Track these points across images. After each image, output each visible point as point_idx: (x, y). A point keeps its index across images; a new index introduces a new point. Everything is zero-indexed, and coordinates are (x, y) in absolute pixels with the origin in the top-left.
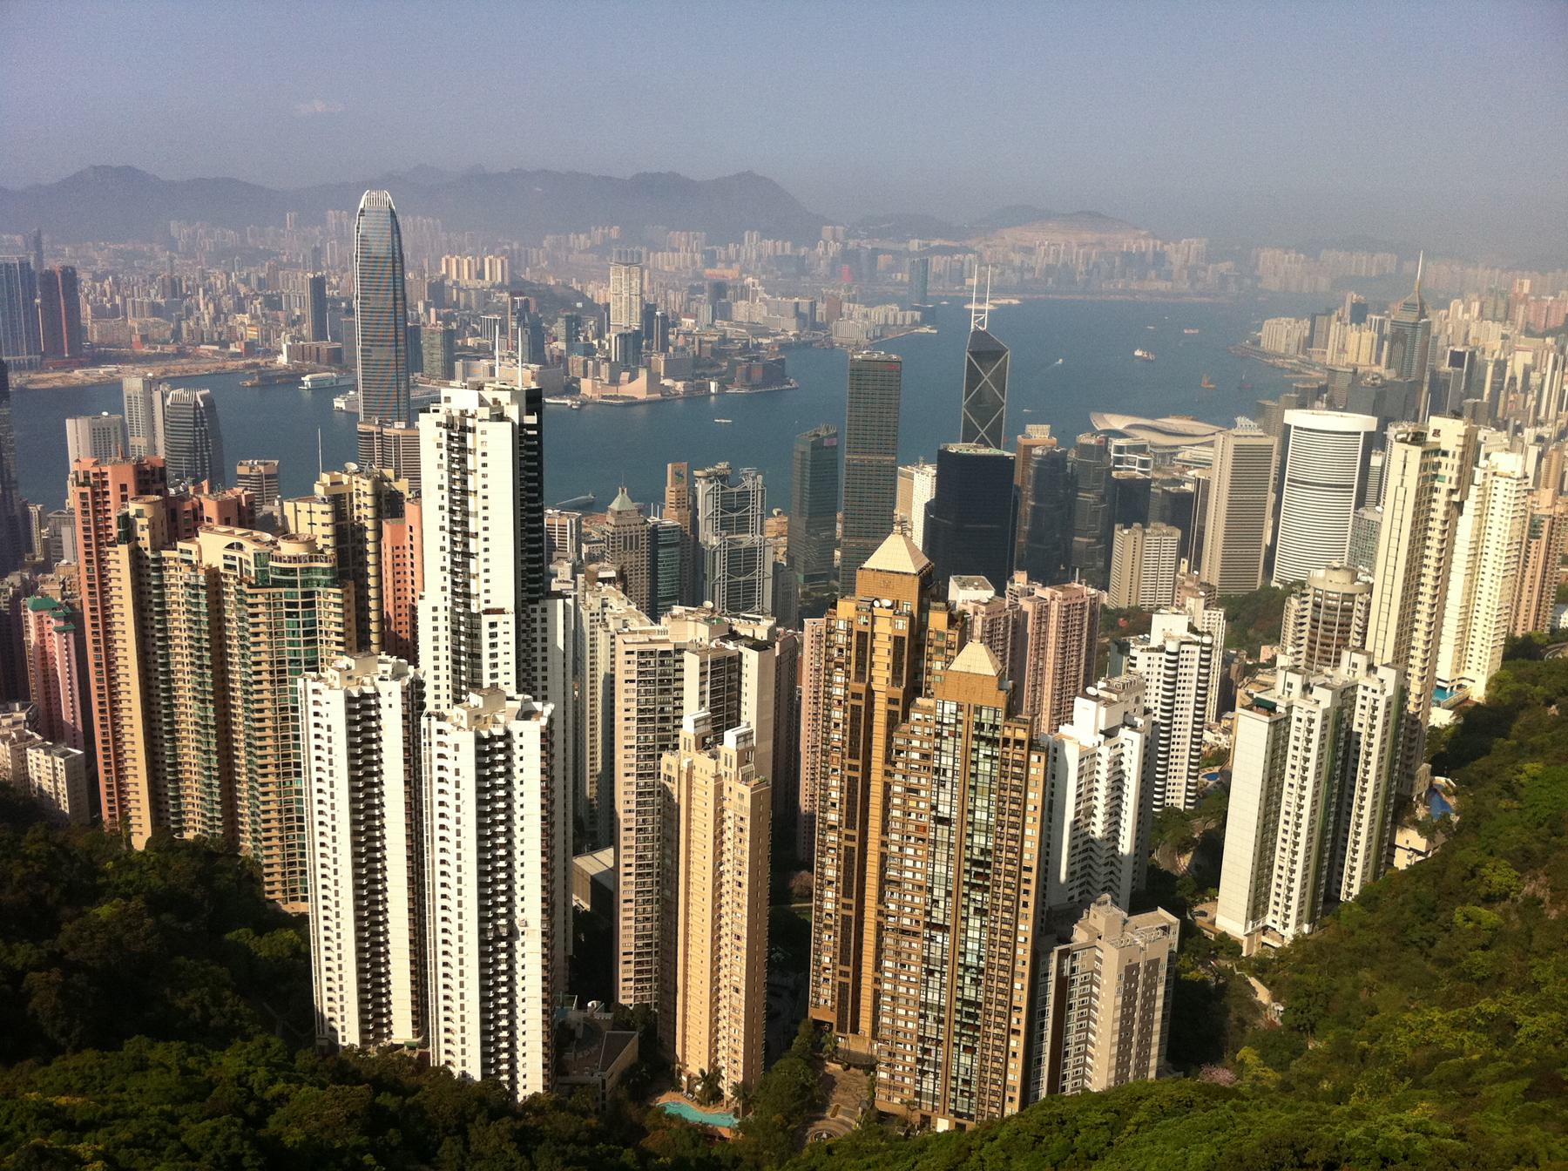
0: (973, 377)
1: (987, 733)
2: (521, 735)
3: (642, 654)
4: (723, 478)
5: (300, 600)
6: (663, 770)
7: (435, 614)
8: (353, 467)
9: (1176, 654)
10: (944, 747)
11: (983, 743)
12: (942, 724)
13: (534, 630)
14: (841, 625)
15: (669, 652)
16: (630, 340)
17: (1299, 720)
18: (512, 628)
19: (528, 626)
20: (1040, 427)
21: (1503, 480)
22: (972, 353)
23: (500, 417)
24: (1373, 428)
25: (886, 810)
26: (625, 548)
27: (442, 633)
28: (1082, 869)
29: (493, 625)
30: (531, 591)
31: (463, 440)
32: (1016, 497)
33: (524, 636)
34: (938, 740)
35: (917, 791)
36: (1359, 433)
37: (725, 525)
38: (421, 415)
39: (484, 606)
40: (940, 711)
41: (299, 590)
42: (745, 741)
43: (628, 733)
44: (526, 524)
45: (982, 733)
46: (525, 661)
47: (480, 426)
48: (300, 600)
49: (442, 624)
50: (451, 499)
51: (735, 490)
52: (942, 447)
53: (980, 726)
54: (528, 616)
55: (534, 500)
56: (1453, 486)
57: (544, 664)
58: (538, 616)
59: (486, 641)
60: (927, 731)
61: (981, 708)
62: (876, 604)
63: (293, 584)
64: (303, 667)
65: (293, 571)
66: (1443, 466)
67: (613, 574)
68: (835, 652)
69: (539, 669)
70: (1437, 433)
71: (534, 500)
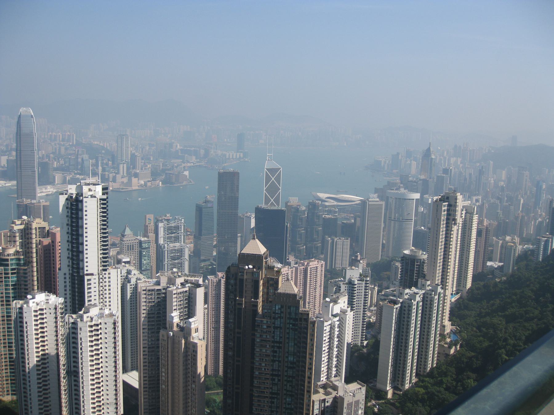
0: (268, 179)
1: (293, 316)
3: (149, 290)
4: (168, 220)
5: (10, 272)
6: (161, 337)
7: (65, 276)
8: (25, 217)
9: (356, 285)
10: (276, 323)
12: (274, 313)
13: (105, 282)
15: (160, 290)
16: (125, 166)
17: (405, 307)
18: (97, 281)
19: (103, 280)
20: (295, 198)
21: (468, 215)
23: (92, 196)
24: (419, 197)
25: (253, 349)
26: (128, 250)
29: (89, 280)
30: (104, 266)
31: (77, 205)
32: (287, 226)
33: (101, 284)
34: (274, 320)
36: (414, 199)
37: (169, 239)
38: (60, 196)
39: (86, 272)
41: (10, 267)
42: (195, 324)
44: (102, 239)
45: (291, 317)
46: (102, 294)
47: (85, 200)
48: (10, 272)
49: (68, 280)
51: (173, 225)
52: (256, 207)
53: (290, 313)
54: (103, 276)
55: (105, 229)
56: (454, 218)
57: (110, 296)
58: (107, 276)
61: (290, 307)
62: (247, 267)
63: (7, 265)
64: (11, 299)
65: (7, 260)
66: (451, 210)
67: (128, 260)
68: (230, 287)
69: (108, 298)
70: (448, 198)
71: (105, 229)
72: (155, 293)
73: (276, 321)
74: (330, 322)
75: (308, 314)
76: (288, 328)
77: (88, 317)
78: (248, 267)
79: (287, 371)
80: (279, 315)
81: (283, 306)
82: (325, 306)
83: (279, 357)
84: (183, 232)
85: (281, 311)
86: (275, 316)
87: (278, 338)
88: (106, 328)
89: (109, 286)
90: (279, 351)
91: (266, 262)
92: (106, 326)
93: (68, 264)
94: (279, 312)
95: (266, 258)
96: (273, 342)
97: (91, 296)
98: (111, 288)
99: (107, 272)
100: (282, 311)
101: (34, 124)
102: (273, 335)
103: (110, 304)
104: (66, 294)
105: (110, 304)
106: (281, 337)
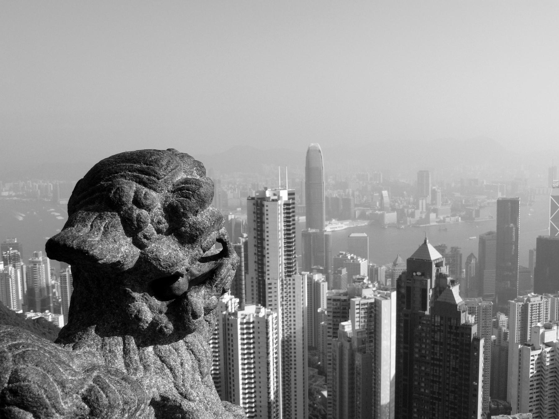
1: (454, 330)
2: (259, 323)
3: (334, 300)
10: (436, 336)
11: (452, 335)
12: (434, 325)
13: (290, 288)
14: (403, 284)
22: (552, 196)
27: (255, 288)
28: (536, 409)
29: (270, 284)
34: (433, 333)
35: (425, 357)
40: (433, 320)
43: (329, 334)
49: (255, 284)
50: (257, 234)
52: (537, 237)
53: (451, 327)
54: (287, 282)
58: (291, 282)
59: (267, 291)
60: (428, 329)
62: (414, 274)
72: (340, 304)
73: (435, 334)
74: (539, 352)
75: (471, 329)
76: (449, 344)
77: (242, 315)
78: (416, 274)
79: (448, 395)
80: (439, 328)
81: (443, 318)
82: (535, 332)
83: (440, 377)
84: (459, 263)
85: (440, 324)
86: (434, 328)
87: (438, 355)
88: (259, 328)
89: (294, 292)
90: (439, 370)
91: (438, 270)
92: (259, 325)
93: (255, 268)
94: (439, 324)
95: (439, 265)
96: (433, 359)
97: (271, 301)
98: (296, 295)
99: (291, 279)
100: (442, 323)
101: (322, 158)
102: (432, 351)
103: (294, 311)
104: (253, 298)
105: (294, 311)
106: (441, 355)
